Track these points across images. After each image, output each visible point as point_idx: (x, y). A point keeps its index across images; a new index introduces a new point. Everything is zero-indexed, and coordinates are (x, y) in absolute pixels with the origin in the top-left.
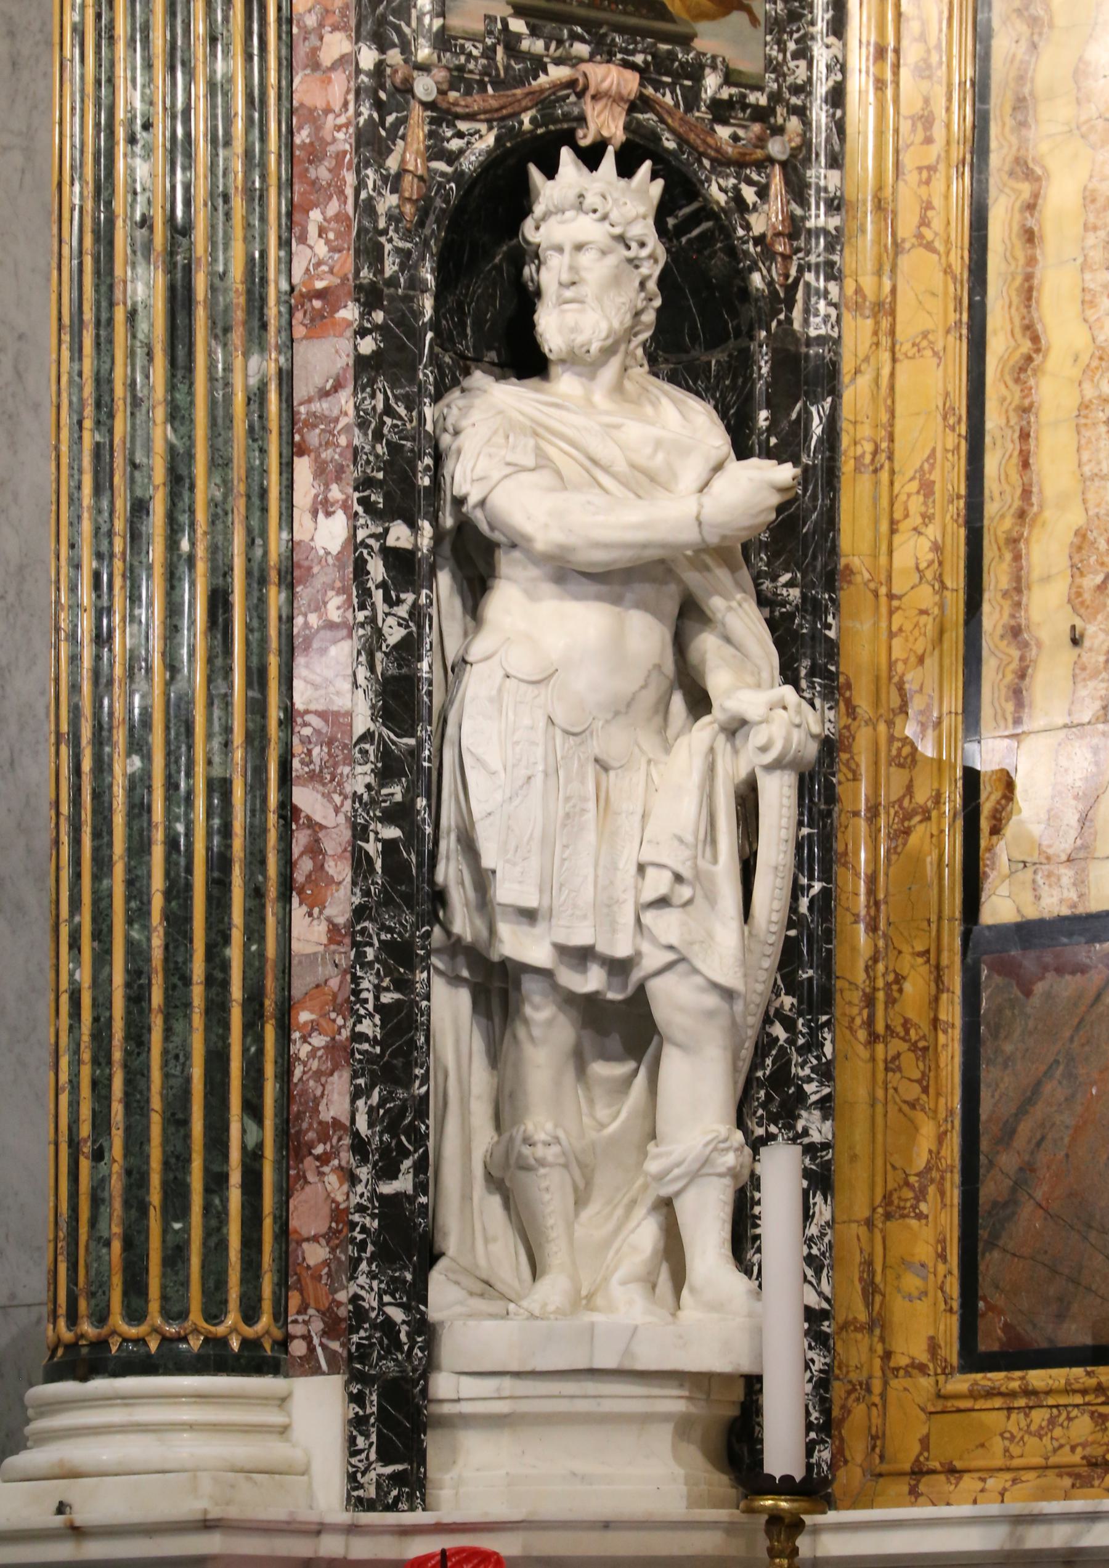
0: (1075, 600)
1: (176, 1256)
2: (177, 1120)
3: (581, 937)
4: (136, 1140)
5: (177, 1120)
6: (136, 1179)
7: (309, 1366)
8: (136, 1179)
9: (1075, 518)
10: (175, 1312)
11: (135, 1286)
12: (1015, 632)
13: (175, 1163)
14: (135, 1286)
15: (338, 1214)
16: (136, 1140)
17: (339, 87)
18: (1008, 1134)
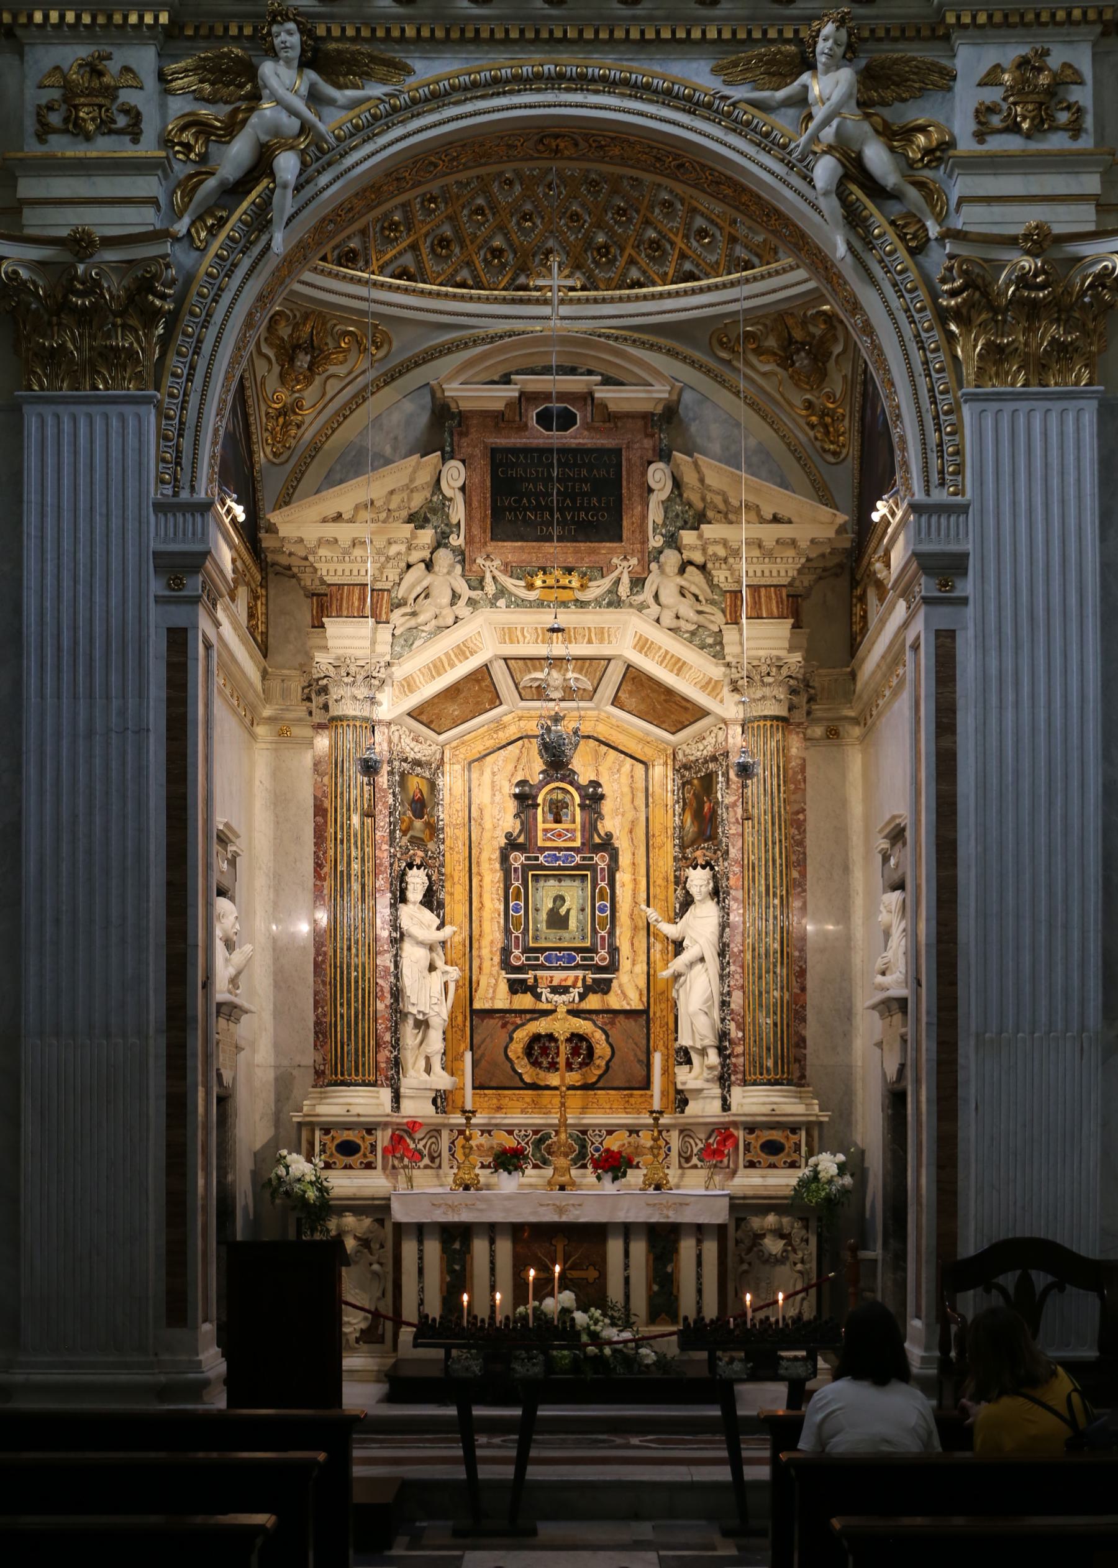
0: (491, 952)
1: (363, 1065)
2: (363, 1040)
3: (422, 1009)
4: (357, 1043)
5: (363, 1040)
6: (357, 1050)
7: (382, 1086)
8: (357, 1050)
9: (491, 938)
10: (364, 1075)
11: (357, 1070)
12: (479, 956)
13: (363, 1047)
14: (357, 1070)
15: (388, 1058)
16: (357, 1043)
17: (386, 854)
18: (479, 1047)
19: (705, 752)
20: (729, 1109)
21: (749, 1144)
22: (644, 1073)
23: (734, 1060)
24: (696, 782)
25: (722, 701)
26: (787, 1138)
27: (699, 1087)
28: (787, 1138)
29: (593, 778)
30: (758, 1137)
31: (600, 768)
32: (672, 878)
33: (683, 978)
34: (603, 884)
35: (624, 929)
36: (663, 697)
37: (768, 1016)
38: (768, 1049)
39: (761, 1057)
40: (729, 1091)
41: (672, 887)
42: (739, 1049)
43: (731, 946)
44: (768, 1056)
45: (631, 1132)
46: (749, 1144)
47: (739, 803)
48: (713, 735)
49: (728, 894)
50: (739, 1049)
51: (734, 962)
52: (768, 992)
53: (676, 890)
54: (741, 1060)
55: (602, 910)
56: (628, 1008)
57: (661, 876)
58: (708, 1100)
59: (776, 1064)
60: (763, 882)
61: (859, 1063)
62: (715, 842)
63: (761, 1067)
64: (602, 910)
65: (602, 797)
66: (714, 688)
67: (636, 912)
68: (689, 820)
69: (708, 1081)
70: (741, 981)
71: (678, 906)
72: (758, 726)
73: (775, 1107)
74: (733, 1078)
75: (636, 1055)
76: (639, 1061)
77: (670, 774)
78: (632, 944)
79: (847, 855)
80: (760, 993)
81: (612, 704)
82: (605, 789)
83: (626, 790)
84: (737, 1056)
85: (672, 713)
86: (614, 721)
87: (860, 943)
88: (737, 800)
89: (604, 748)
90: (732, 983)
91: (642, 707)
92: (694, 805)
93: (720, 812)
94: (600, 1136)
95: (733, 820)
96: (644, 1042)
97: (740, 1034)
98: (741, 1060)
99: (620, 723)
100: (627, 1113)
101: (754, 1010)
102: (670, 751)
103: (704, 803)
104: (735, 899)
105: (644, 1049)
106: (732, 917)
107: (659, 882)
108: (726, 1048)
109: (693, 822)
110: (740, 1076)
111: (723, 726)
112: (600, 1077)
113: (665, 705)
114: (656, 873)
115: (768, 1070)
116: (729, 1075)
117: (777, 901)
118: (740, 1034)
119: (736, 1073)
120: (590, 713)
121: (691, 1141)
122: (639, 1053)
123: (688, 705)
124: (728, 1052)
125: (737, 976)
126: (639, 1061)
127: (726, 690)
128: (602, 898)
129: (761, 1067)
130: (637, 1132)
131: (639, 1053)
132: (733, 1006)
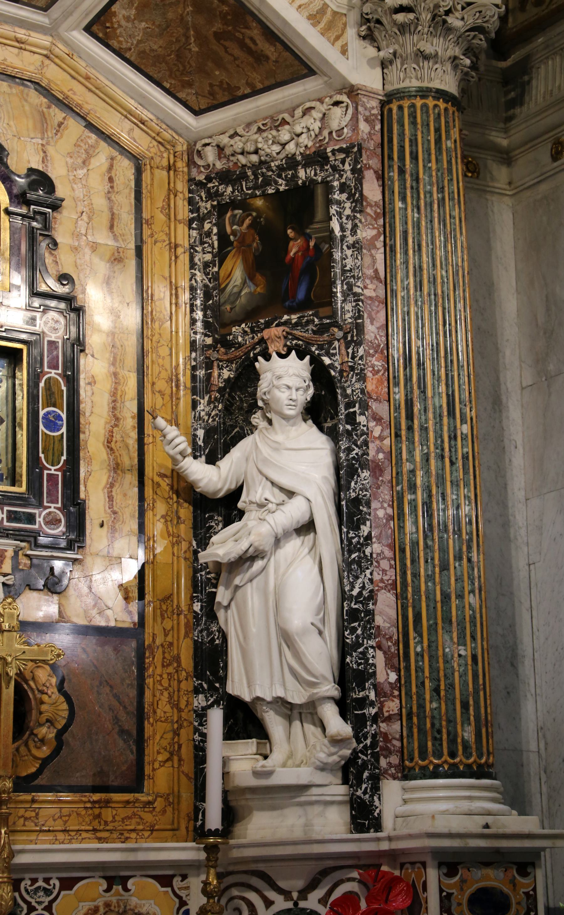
19: (291, 148)
20: (377, 825)
21: (449, 895)
22: (132, 757)
23: (383, 726)
24: (259, 202)
25: (344, 51)
26: (513, 883)
27: (303, 780)
28: (513, 882)
29: (36, 164)
30: (463, 881)
31: (51, 150)
32: (185, 379)
33: (258, 565)
34: (53, 373)
35: (95, 466)
36: (218, 26)
37: (462, 641)
38: (465, 706)
39: (451, 721)
40: (376, 789)
41: (185, 397)
42: (392, 706)
43: (374, 505)
44: (466, 720)
45: (111, 881)
46: (449, 895)
47: (380, 244)
48: (317, 115)
49: (365, 407)
50: (392, 706)
51: (379, 538)
52: (460, 597)
53: (195, 404)
54: (396, 726)
55: (52, 424)
56: (103, 624)
57: (164, 375)
58: (317, 809)
59: (478, 735)
60: (443, 388)
61: (533, 746)
62: (324, 311)
63: (453, 740)
64: (52, 424)
65: (56, 206)
66: (329, 27)
67: (117, 436)
68: (238, 275)
69: (323, 768)
70: (391, 574)
71: (201, 433)
72: (425, 106)
73: (489, 819)
74: (383, 762)
75: (116, 719)
76: (122, 732)
77: (181, 186)
78: (111, 498)
79: (498, 379)
80: (446, 597)
81: (88, 29)
82: (61, 191)
83: (100, 202)
84: (389, 719)
85: (219, 64)
86: (81, 66)
87: (523, 532)
88: (376, 238)
89: (57, 114)
90: (376, 577)
91: (156, 45)
92: (256, 244)
93: (337, 255)
94: (48, 892)
95: (370, 272)
96: (133, 693)
97: (393, 677)
98: (396, 726)
99: (92, 72)
100: (100, 840)
101: (433, 629)
102: (181, 147)
103: (288, 240)
104: (378, 419)
105: (132, 708)
106: (372, 452)
107: (161, 385)
108: (363, 702)
109: (250, 275)
110: (395, 759)
111: (344, 98)
112: (45, 762)
113: (215, 46)
114: (156, 369)
115: (466, 746)
116: (376, 757)
117: (466, 429)
118: (393, 677)
119: (388, 752)
120: (38, 38)
121: (253, 896)
122: (123, 716)
123: (269, 50)
124: (373, 711)
125: (385, 564)
126: (122, 732)
127: (351, 33)
128: (51, 402)
129: (453, 740)
130: (124, 881)
131: (123, 716)
132: (379, 620)
